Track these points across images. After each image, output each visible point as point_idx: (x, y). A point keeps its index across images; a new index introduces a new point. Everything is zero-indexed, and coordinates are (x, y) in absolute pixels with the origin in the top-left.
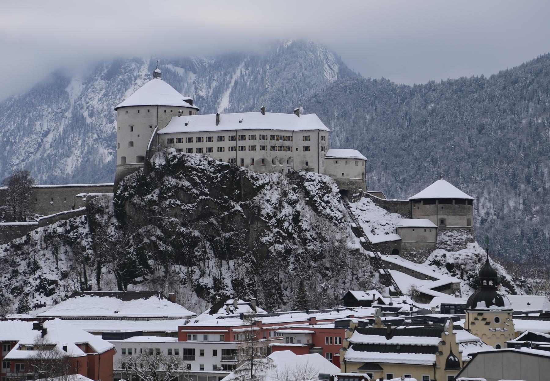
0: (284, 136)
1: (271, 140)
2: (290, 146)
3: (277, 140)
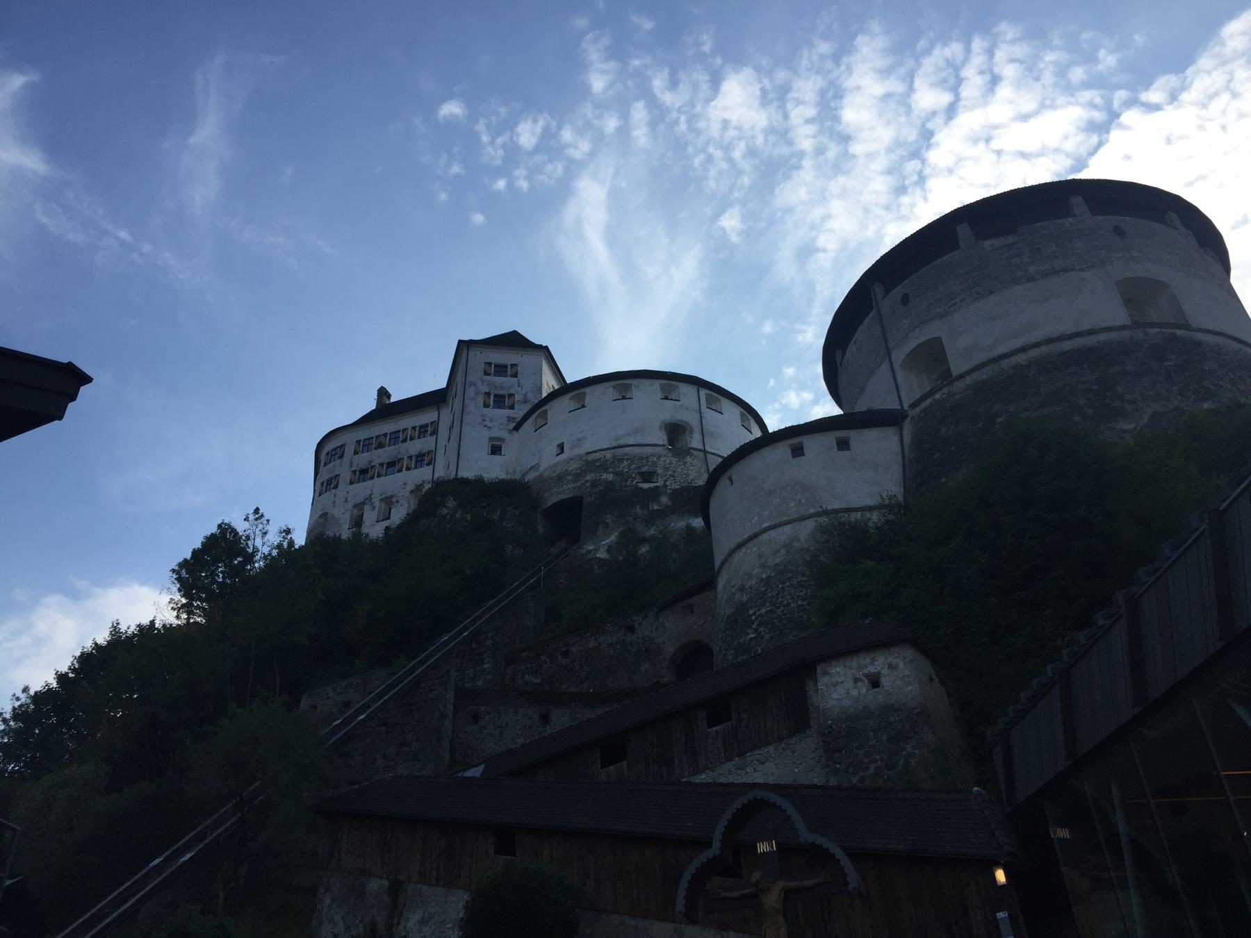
0: (404, 430)
1: (356, 453)
2: (426, 449)
3: (380, 446)
